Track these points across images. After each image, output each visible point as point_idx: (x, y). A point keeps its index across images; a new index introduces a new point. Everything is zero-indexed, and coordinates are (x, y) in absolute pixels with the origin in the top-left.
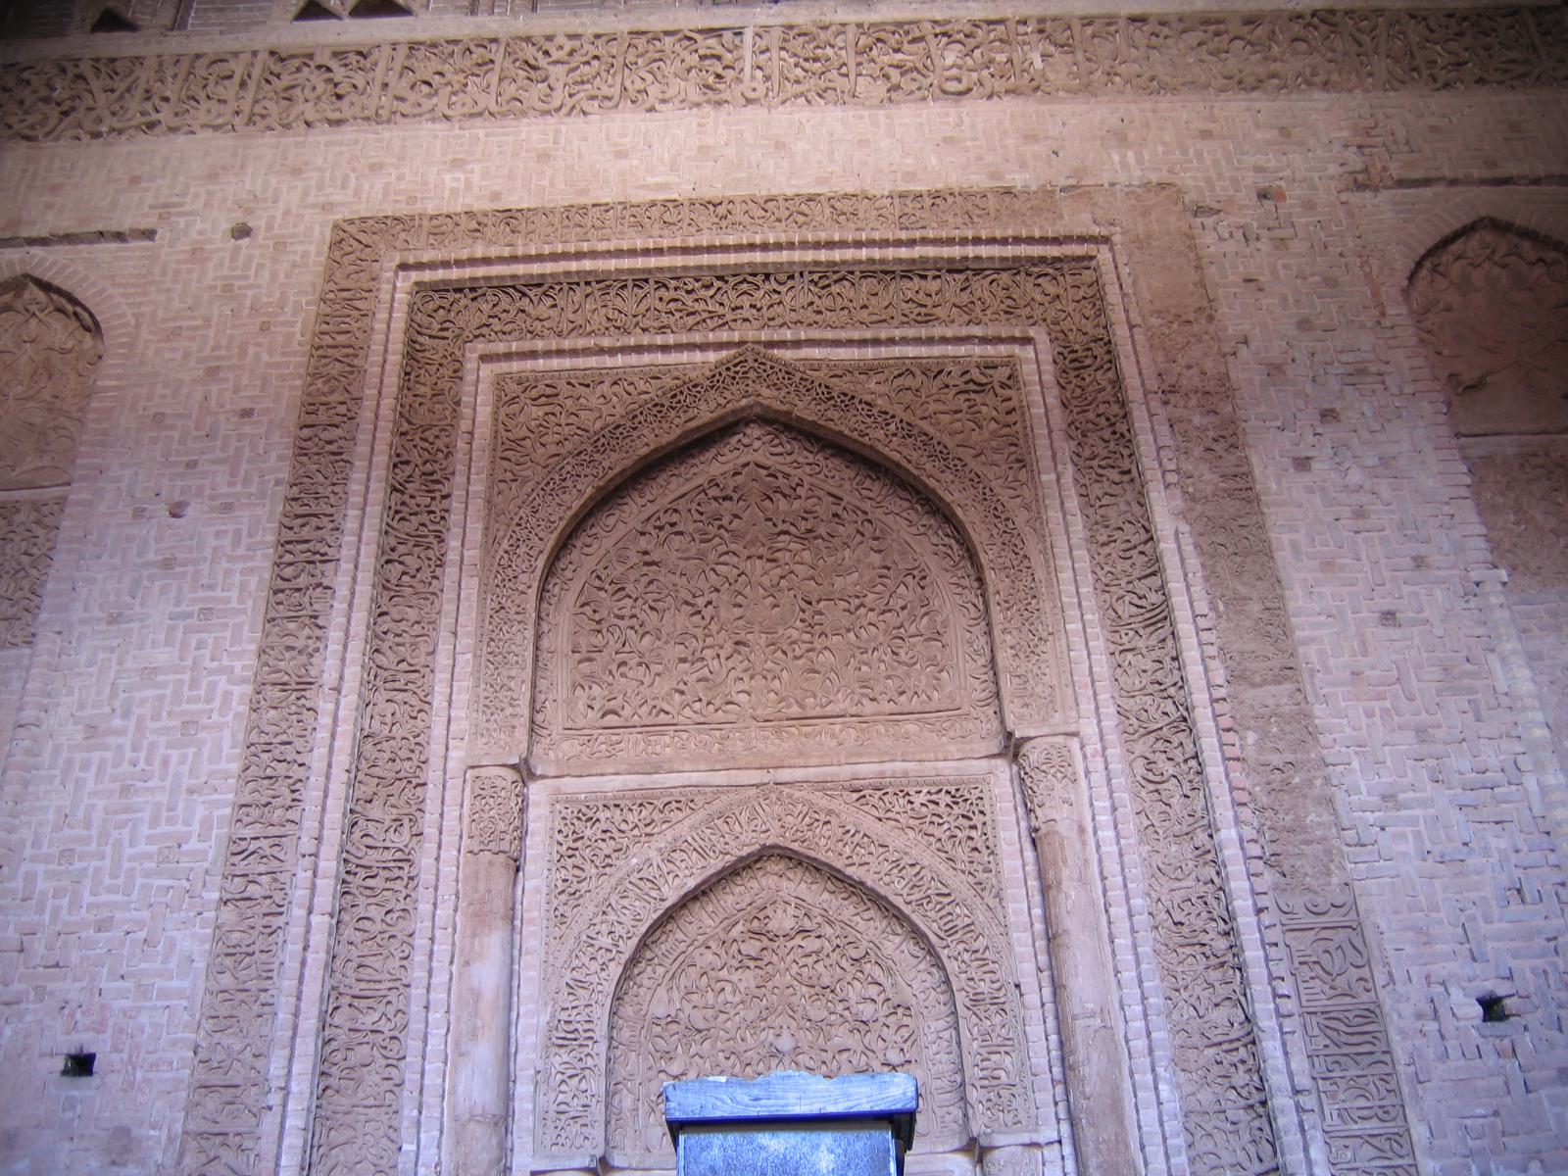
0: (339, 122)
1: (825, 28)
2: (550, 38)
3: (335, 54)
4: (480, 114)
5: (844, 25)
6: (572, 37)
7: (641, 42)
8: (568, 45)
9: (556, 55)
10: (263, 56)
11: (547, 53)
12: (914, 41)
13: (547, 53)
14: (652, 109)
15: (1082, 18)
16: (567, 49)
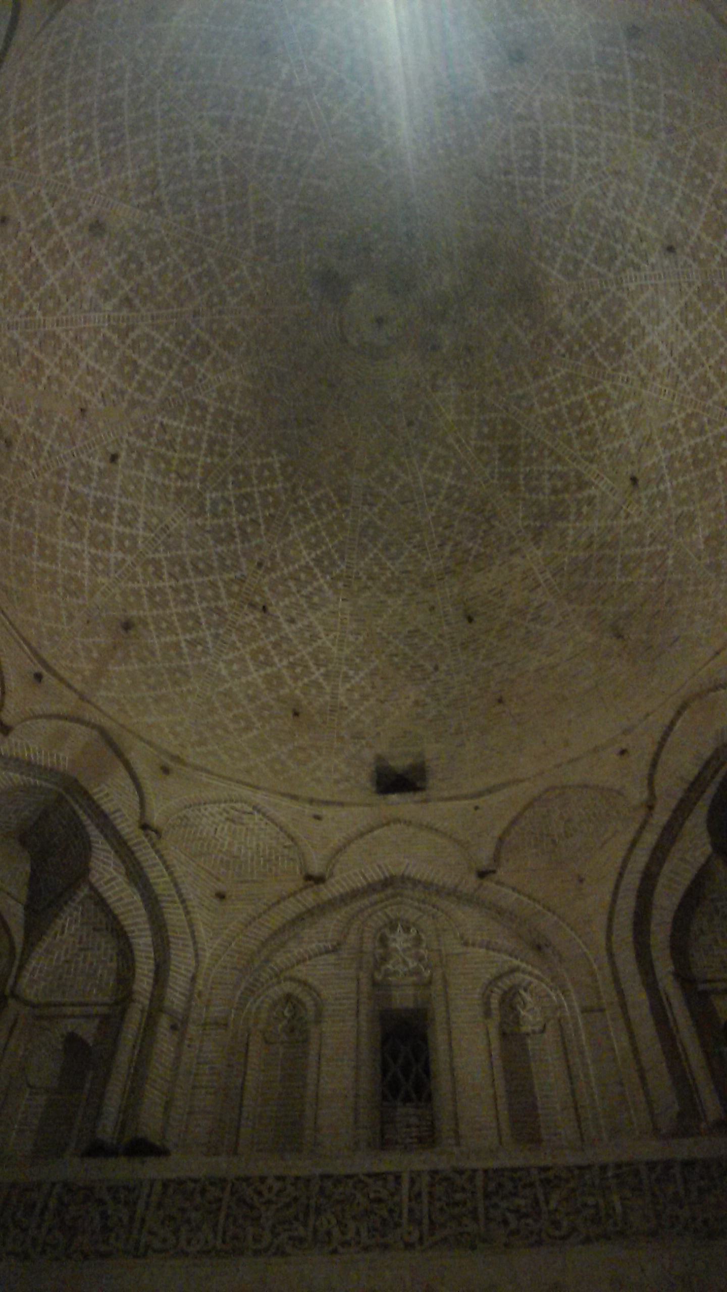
0: (105, 1256)
1: (461, 1172)
2: (263, 1179)
3: (109, 1189)
4: (209, 1252)
5: (475, 1171)
6: (279, 1178)
7: (329, 1184)
8: (277, 1186)
9: (267, 1196)
10: (57, 1189)
11: (260, 1194)
12: (524, 1186)
13: (260, 1194)
14: (335, 1252)
15: (647, 1163)
16: (275, 1190)
